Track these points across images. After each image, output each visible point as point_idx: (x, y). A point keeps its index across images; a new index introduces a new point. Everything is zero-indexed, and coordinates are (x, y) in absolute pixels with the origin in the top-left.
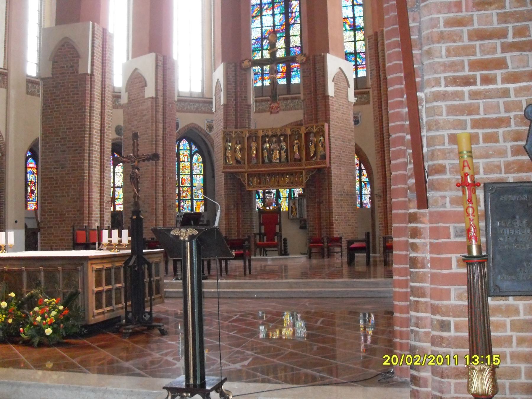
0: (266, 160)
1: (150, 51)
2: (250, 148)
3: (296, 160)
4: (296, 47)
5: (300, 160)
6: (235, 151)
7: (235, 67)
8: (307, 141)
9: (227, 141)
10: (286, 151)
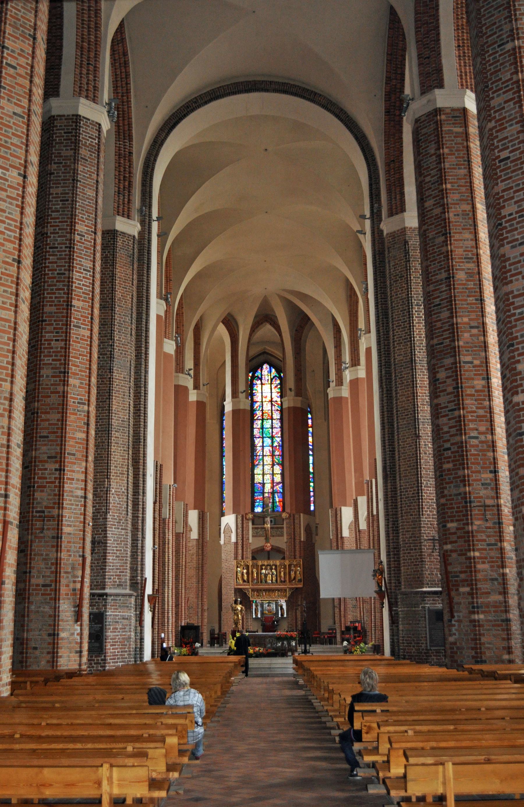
0: (264, 581)
1: (195, 509)
2: (252, 572)
3: (281, 581)
4: (259, 483)
5: (284, 582)
6: (243, 575)
7: (242, 516)
8: (290, 571)
9: (237, 567)
10: (276, 576)
